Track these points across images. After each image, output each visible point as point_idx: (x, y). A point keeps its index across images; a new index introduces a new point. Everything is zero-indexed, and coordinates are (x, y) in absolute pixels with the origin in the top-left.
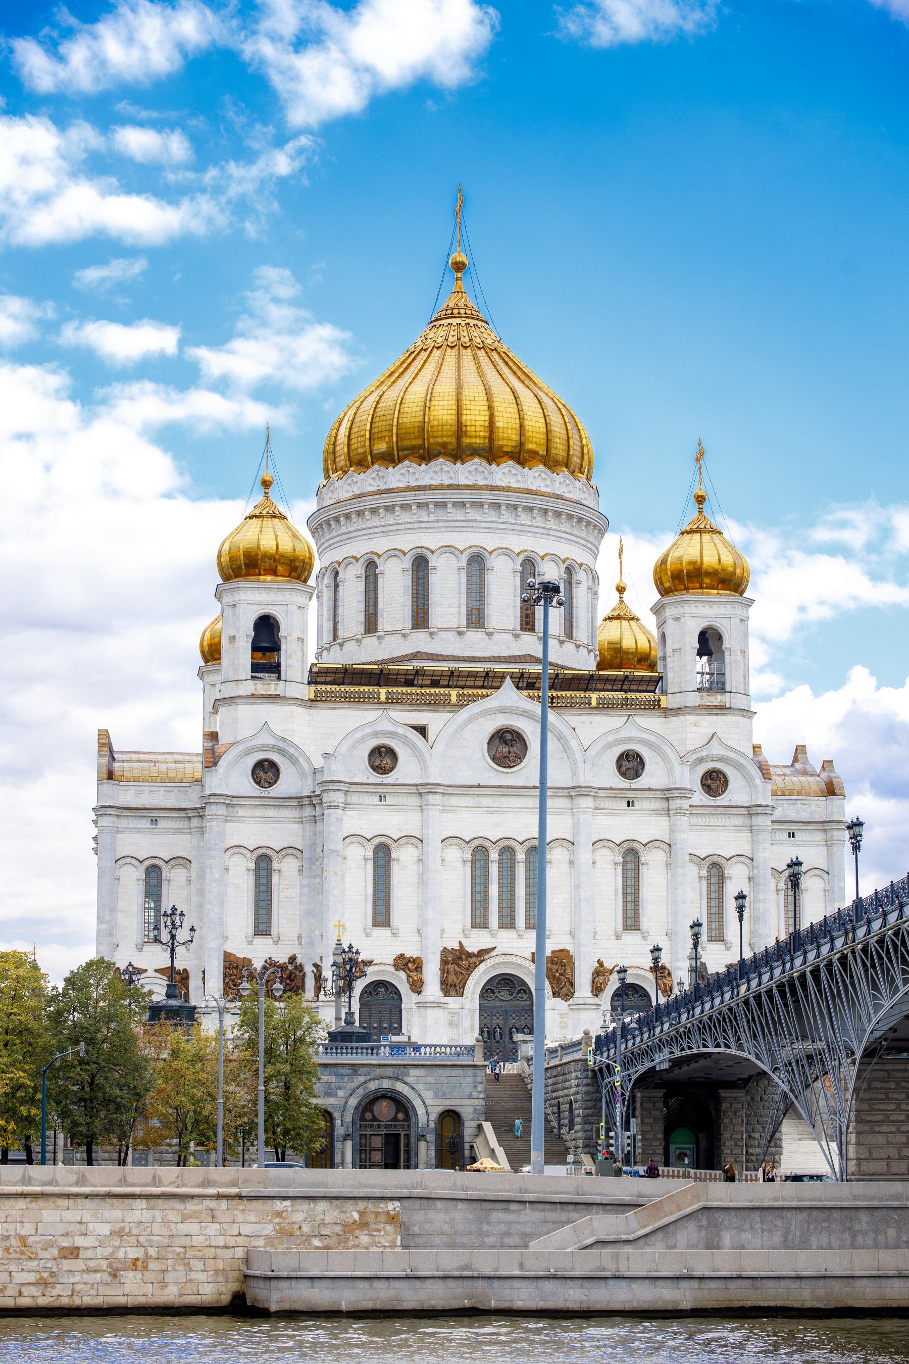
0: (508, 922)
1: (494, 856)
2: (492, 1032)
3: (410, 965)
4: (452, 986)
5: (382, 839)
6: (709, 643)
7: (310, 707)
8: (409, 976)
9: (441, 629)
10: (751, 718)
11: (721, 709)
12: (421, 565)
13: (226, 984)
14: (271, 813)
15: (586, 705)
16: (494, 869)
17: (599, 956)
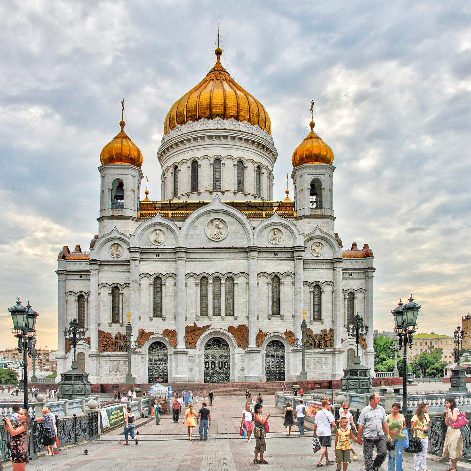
0: (217, 314)
1: (210, 281)
2: (210, 363)
3: (171, 334)
4: (190, 343)
5: (158, 275)
6: (315, 188)
7: (138, 221)
8: (170, 339)
9: (203, 192)
10: (334, 220)
11: (321, 216)
12: (195, 165)
13: (99, 344)
14: (119, 268)
15: (260, 216)
16: (211, 288)
17: (260, 328)
